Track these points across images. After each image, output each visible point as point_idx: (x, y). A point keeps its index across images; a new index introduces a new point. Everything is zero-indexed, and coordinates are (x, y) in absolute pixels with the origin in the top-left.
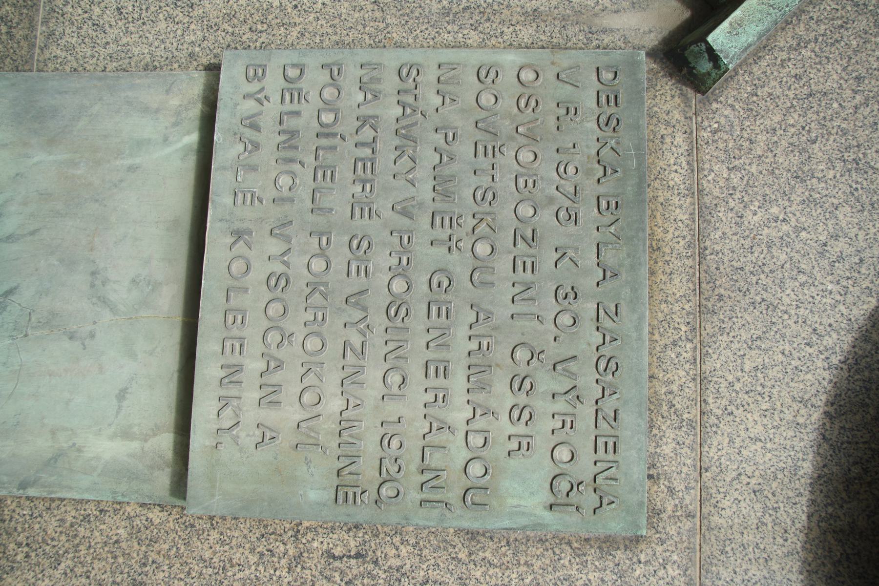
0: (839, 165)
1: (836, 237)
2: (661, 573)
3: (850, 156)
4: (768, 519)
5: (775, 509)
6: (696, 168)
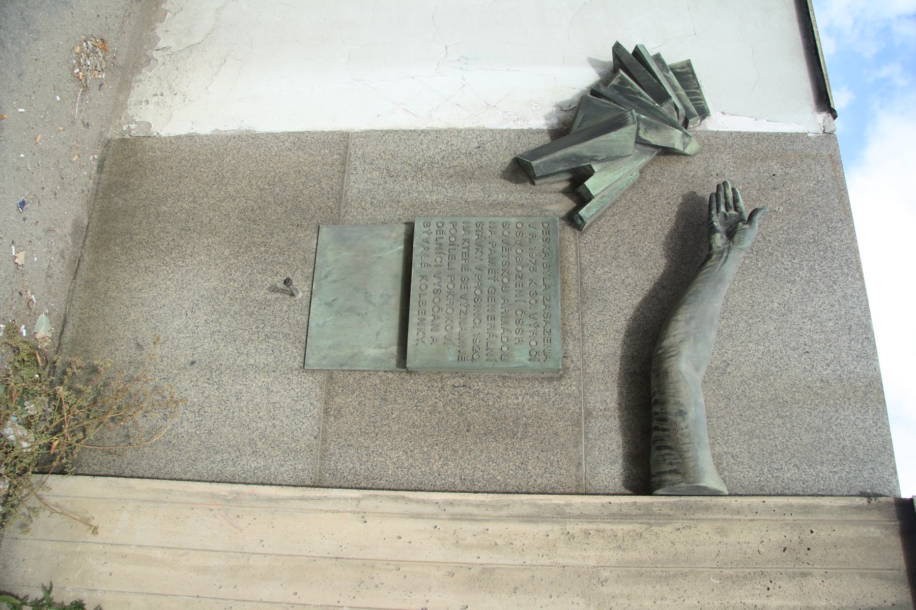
3: (632, 251)
6: (578, 255)
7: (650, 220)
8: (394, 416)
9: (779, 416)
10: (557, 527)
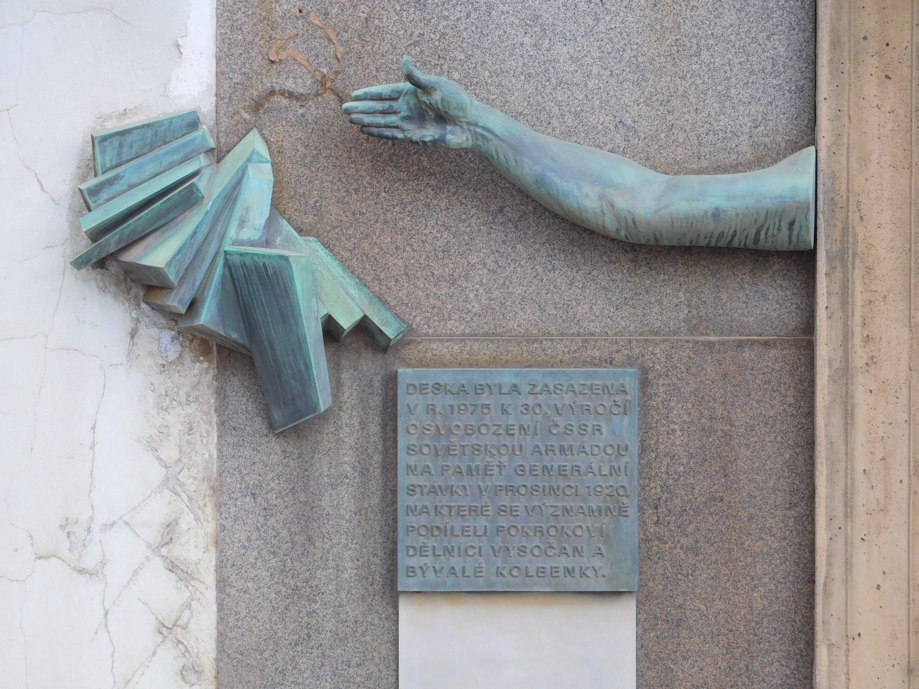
0: (446, 261)
1: (485, 264)
2: (658, 356)
3: (441, 255)
4: (630, 303)
5: (626, 299)
6: (451, 338)
7: (386, 222)
8: (703, 607)
9: (698, 54)
10: (860, 379)
